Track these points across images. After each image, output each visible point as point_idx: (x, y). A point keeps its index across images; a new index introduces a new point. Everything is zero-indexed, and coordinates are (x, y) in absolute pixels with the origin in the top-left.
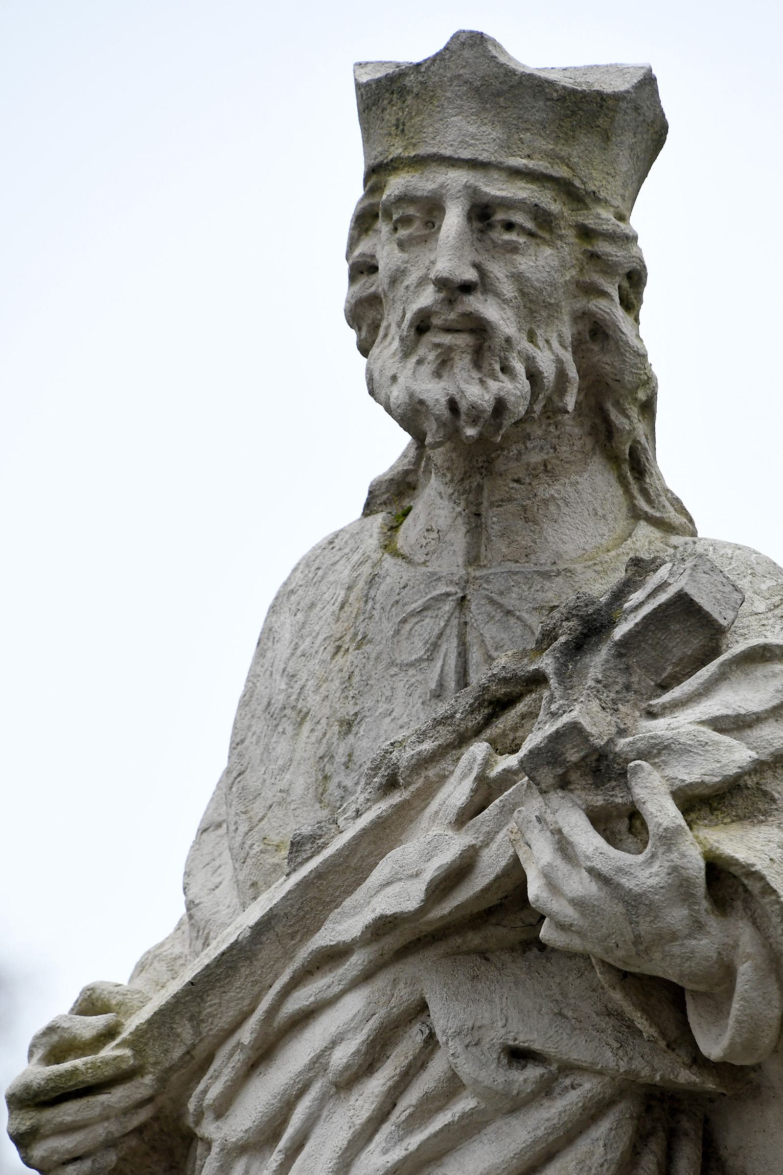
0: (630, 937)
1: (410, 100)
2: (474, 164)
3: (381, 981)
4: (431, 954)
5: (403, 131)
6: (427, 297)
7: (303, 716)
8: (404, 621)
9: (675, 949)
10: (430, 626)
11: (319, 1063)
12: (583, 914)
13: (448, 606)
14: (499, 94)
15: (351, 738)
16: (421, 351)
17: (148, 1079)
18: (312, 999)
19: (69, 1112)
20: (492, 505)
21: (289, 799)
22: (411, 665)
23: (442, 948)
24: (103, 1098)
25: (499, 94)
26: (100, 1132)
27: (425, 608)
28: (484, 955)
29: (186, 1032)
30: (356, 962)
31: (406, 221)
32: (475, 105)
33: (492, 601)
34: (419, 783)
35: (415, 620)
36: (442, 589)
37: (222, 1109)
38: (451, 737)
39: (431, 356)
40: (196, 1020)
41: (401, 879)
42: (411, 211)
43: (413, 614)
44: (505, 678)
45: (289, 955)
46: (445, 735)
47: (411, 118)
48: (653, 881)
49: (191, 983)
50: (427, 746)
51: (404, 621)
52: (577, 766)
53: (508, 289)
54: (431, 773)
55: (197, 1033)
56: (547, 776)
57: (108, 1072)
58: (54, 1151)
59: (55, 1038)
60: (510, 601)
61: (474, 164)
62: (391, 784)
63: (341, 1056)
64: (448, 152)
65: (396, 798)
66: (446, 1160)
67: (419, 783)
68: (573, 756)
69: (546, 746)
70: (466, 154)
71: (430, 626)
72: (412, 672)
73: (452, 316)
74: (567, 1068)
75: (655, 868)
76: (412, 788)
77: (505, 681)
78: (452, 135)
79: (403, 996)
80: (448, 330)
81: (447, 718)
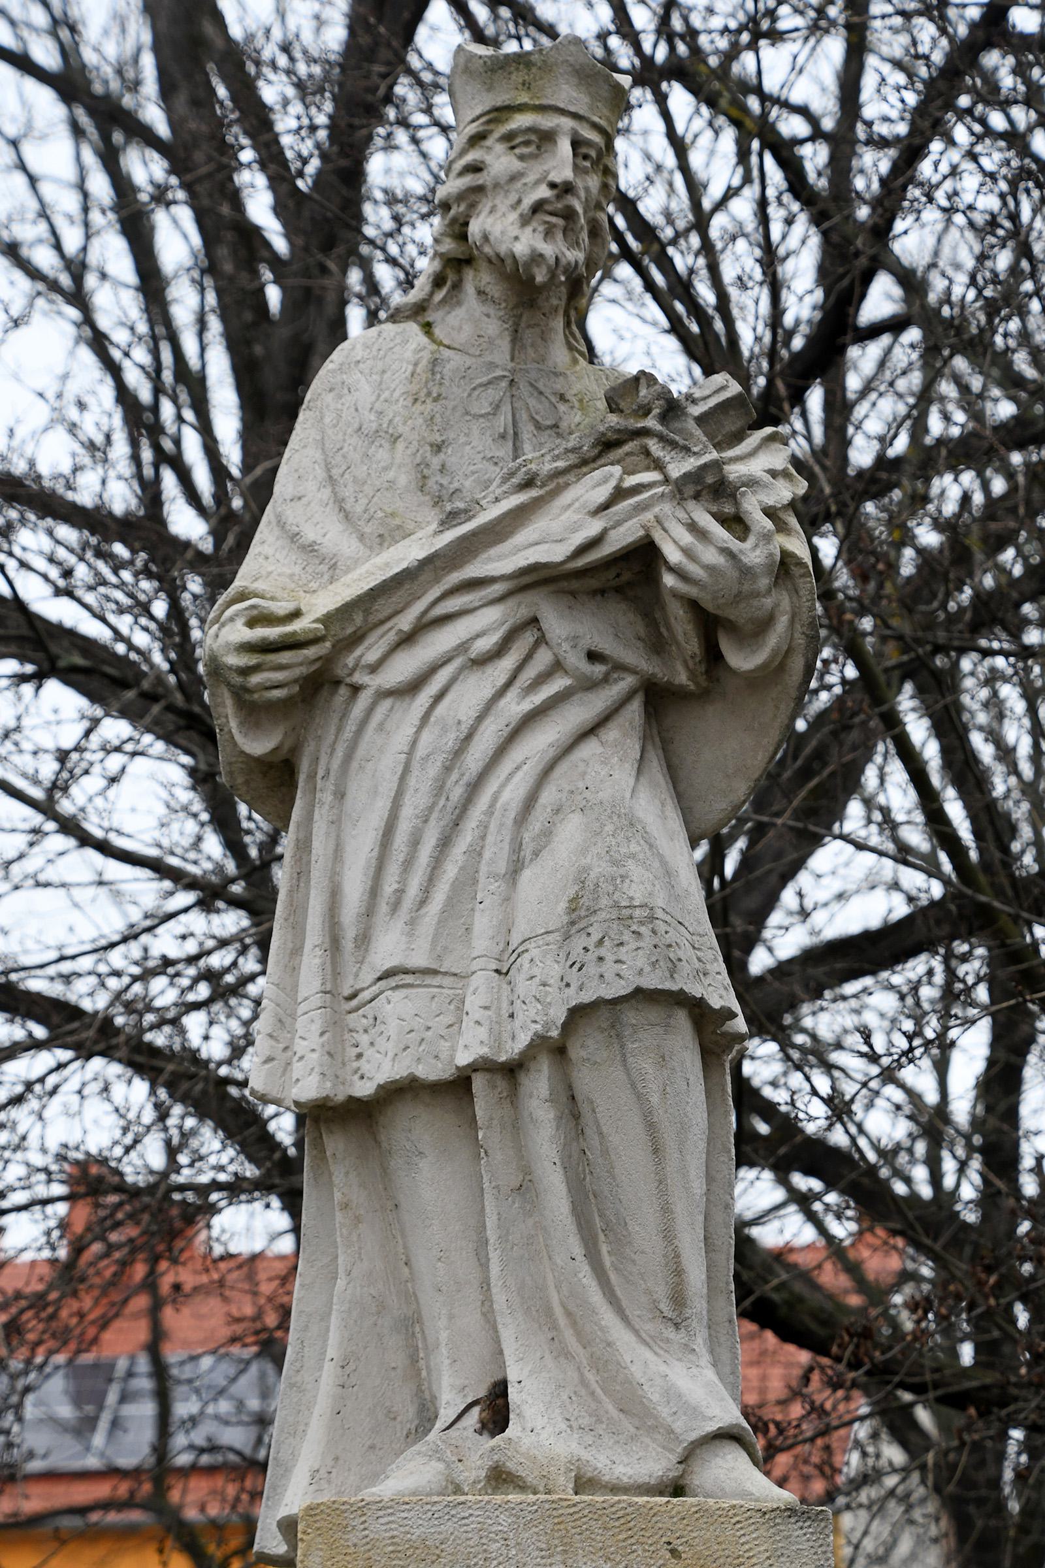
0: (735, 591)
1: (534, 70)
2: (576, 116)
3: (511, 603)
4: (544, 590)
6: (544, 192)
7: (395, 439)
8: (474, 389)
9: (755, 603)
10: (493, 394)
11: (463, 647)
13: (504, 384)
14: (588, 76)
15: (442, 456)
16: (534, 224)
17: (328, 644)
19: (285, 657)
20: (529, 326)
22: (482, 416)
23: (552, 587)
24: (305, 652)
25: (588, 76)
26: (303, 671)
27: (490, 383)
28: (573, 594)
29: (358, 619)
30: (498, 589)
31: (527, 143)
32: (575, 80)
33: (531, 385)
34: (551, 486)
36: (499, 373)
37: (374, 669)
38: (577, 461)
39: (541, 228)
40: (367, 612)
42: (533, 137)
43: (481, 385)
45: (437, 580)
46: (573, 459)
48: (758, 560)
50: (561, 464)
51: (474, 389)
52: (710, 486)
53: (582, 194)
54: (561, 480)
55: (365, 620)
56: (690, 490)
57: (311, 636)
58: (269, 680)
59: (255, 612)
60: (540, 385)
61: (576, 116)
62: (528, 484)
63: (485, 644)
64: (562, 105)
65: (534, 493)
66: (551, 712)
67: (551, 486)
68: (710, 480)
70: (572, 109)
71: (493, 394)
73: (559, 206)
74: (620, 667)
75: (758, 552)
76: (547, 488)
77: (619, 431)
78: (564, 95)
79: (523, 613)
80: (551, 214)
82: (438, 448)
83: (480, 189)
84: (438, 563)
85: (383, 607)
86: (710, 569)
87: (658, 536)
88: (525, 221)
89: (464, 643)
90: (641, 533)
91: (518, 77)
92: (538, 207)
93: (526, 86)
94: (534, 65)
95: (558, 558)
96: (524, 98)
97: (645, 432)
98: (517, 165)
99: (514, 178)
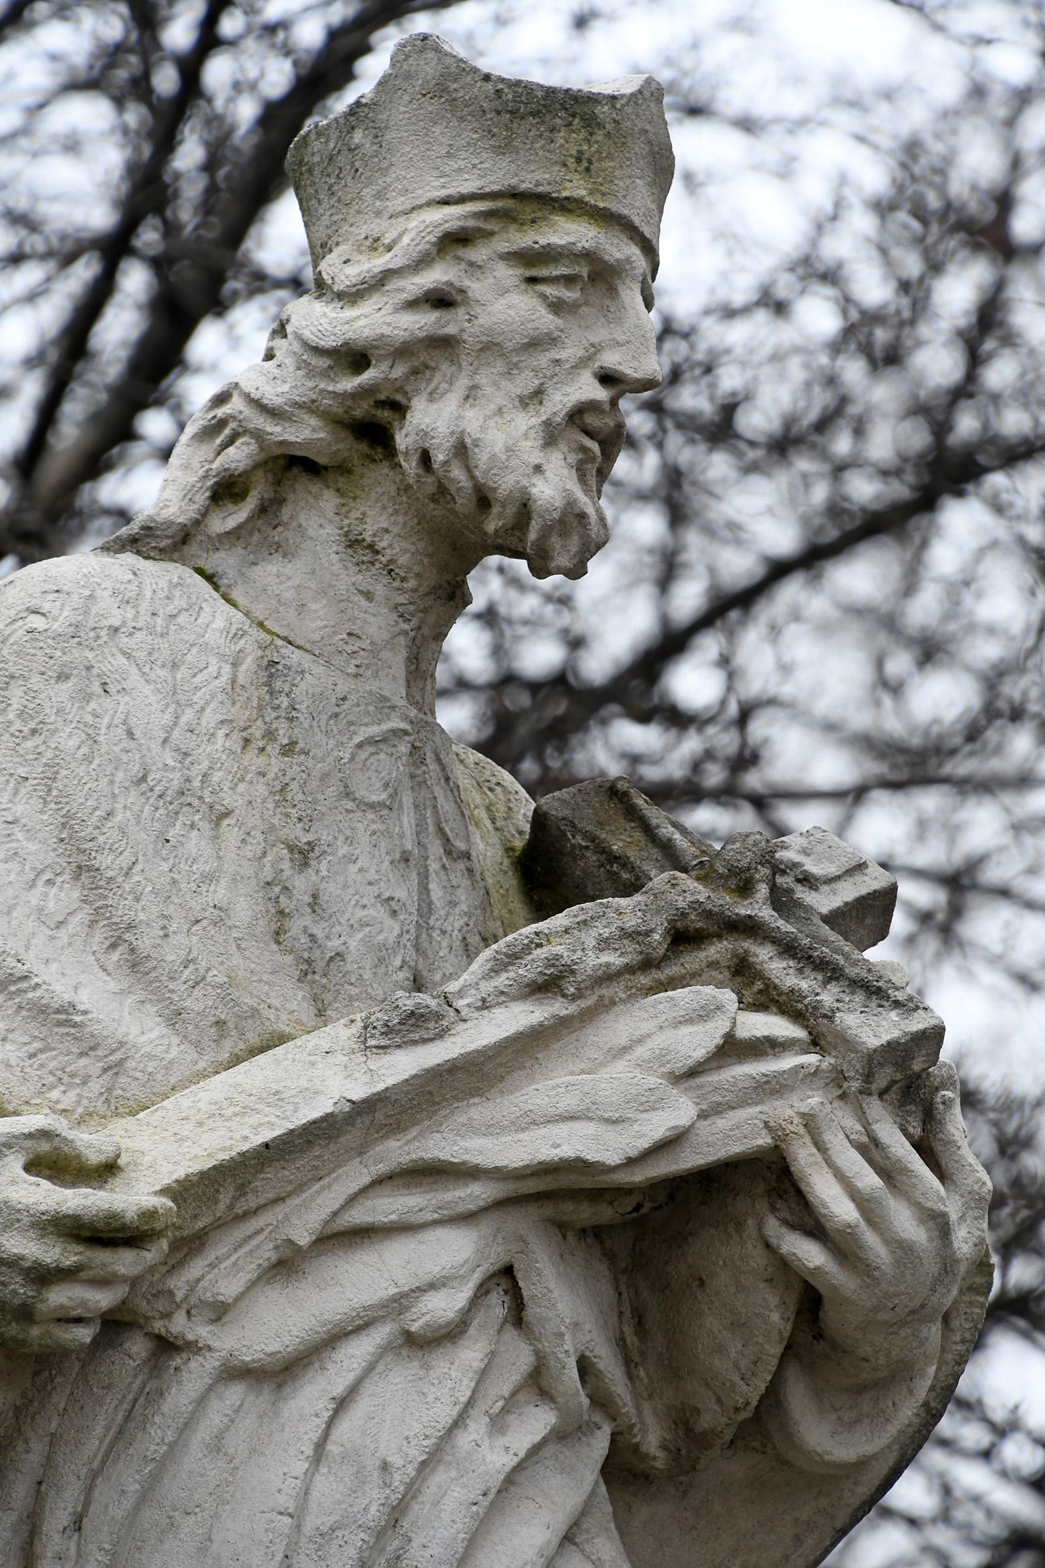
1: (599, 135)
5: (588, 170)
11: (399, 1303)
12: (897, 1263)
18: (393, 1217)
21: (229, 923)
22: (372, 806)
23: (549, 1210)
30: (477, 1193)
35: (372, 750)
37: (220, 1312)
41: (591, 1119)
44: (710, 911)
47: (600, 160)
49: (266, 1145)
69: (906, 1043)
72: (370, 815)
81: (639, 933)
82: (303, 855)
83: (444, 344)
84: (379, 1116)
85: (267, 1184)
86: (902, 1249)
87: (803, 1157)
88: (550, 436)
89: (403, 1295)
90: (764, 1140)
91: (569, 141)
92: (578, 415)
93: (584, 164)
94: (600, 126)
95: (612, 1158)
96: (576, 188)
97: (751, 928)
98: (547, 320)
99: (536, 343)
